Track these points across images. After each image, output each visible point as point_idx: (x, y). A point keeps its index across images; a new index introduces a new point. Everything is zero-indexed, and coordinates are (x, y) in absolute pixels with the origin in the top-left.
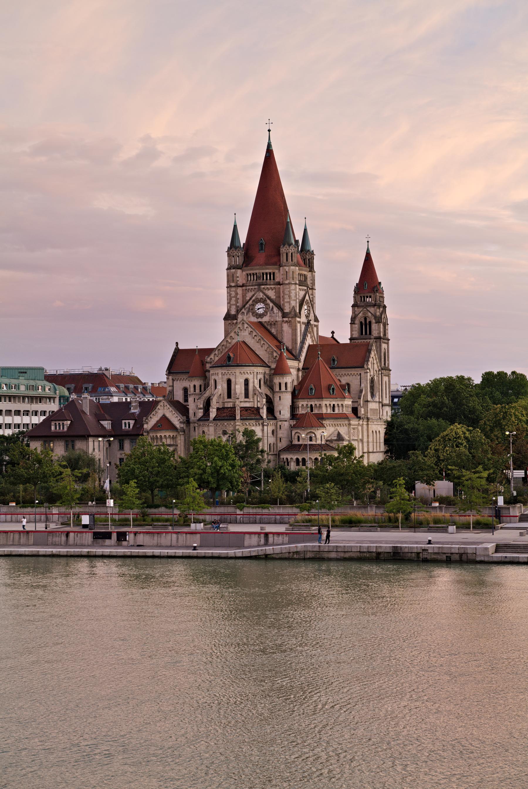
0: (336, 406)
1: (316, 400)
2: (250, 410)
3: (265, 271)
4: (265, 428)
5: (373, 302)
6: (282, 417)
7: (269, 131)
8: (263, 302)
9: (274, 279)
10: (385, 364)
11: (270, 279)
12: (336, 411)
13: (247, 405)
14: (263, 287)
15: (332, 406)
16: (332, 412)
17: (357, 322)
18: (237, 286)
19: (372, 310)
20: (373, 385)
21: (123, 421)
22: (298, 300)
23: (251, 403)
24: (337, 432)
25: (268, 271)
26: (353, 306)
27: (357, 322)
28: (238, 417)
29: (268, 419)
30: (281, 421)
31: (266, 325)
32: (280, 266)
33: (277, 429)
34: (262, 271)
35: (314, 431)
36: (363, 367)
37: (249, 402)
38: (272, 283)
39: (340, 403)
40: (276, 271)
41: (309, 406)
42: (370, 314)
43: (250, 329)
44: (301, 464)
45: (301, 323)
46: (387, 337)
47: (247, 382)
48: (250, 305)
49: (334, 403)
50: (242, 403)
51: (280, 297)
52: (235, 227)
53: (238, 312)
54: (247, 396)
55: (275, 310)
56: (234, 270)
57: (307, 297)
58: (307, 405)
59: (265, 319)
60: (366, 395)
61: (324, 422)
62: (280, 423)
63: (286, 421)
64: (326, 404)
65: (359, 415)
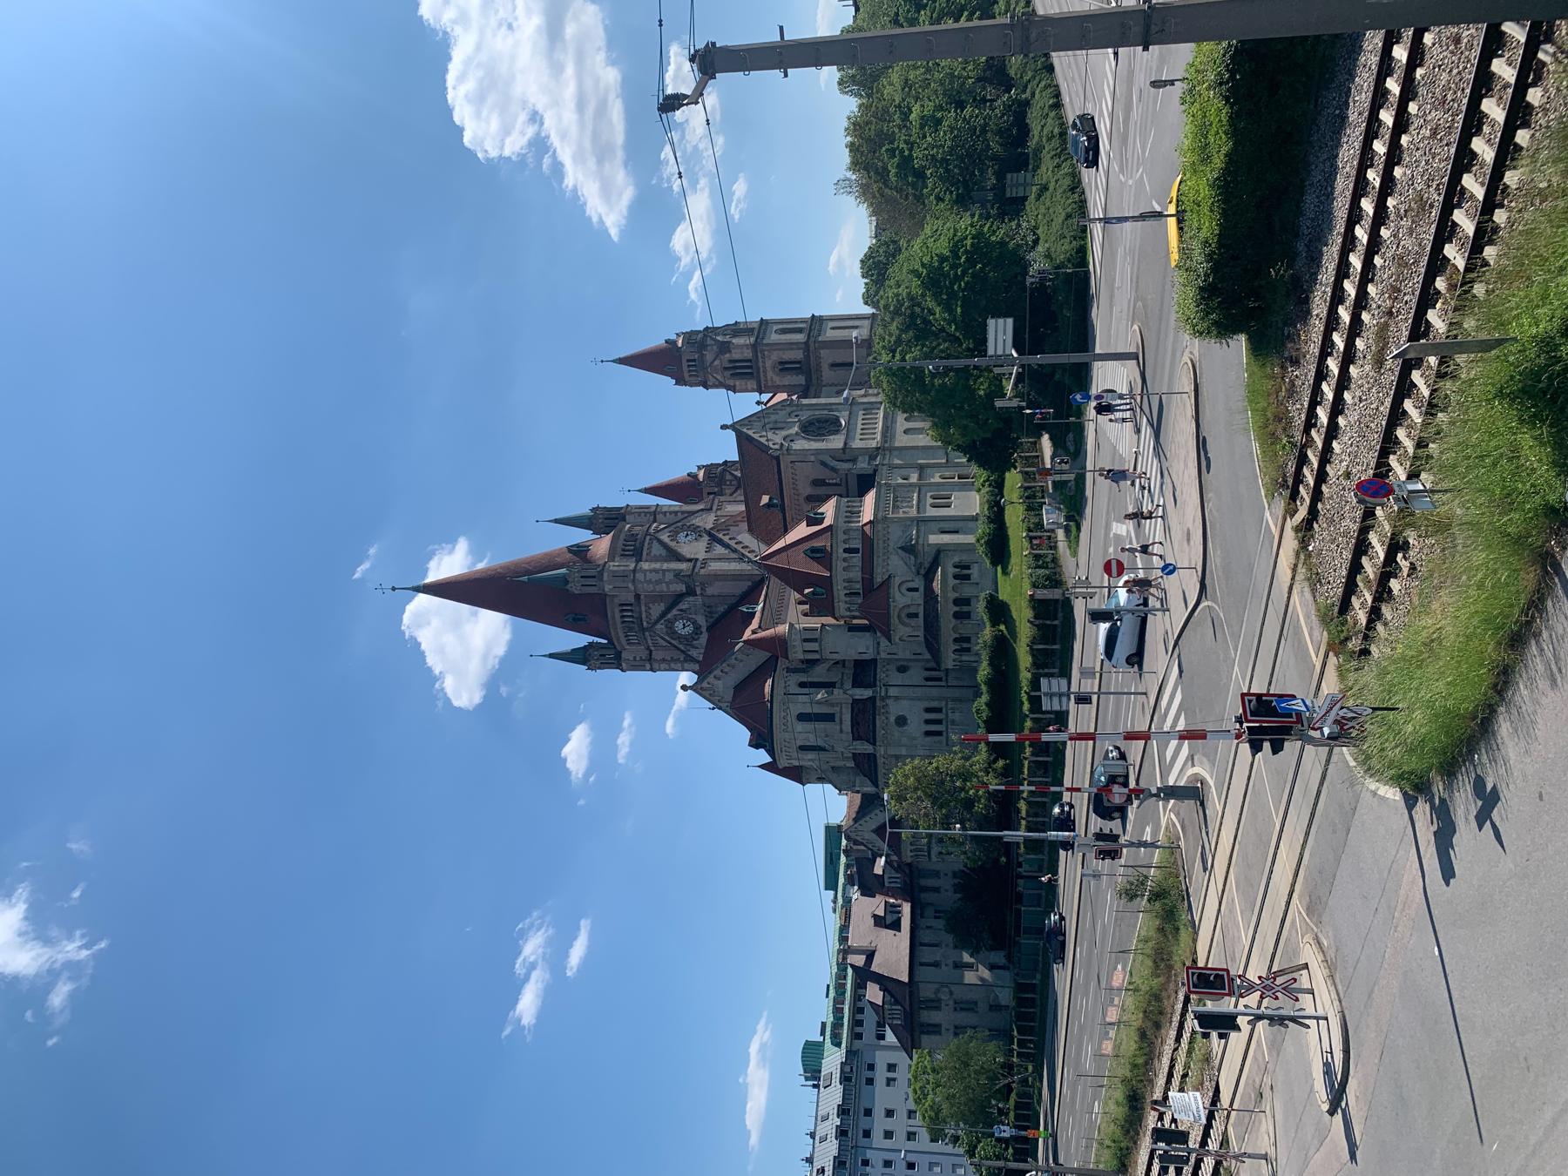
0: (847, 546)
1: (835, 589)
2: (857, 715)
3: (618, 620)
4: (893, 692)
5: (696, 356)
6: (871, 650)
7: (394, 589)
8: (673, 623)
9: (631, 605)
10: (800, 331)
11: (631, 611)
12: (860, 546)
13: (847, 717)
14: (645, 624)
15: (847, 555)
16: (860, 555)
17: (731, 382)
18: (650, 659)
19: (709, 356)
20: (819, 421)
21: (887, 884)
22: (665, 566)
23: (844, 710)
24: (900, 551)
25: (618, 615)
26: (706, 387)
27: (731, 382)
28: (868, 748)
29: (875, 686)
30: (878, 653)
31: (711, 620)
32: (606, 595)
33: (897, 660)
34: (619, 625)
35: (896, 614)
36: (777, 458)
37: (841, 713)
38: (637, 609)
39: (842, 537)
40: (617, 601)
41: (848, 599)
42: (717, 362)
43: (711, 679)
44: (965, 645)
45: (709, 555)
46: (756, 326)
47: (802, 717)
48: (681, 643)
49: (841, 550)
50: (844, 728)
51: (660, 597)
52: (551, 656)
53: (693, 660)
54: (829, 718)
55: (683, 606)
56: (624, 665)
57: (665, 537)
58: (846, 602)
59: (702, 621)
60: (833, 454)
61: (879, 579)
62: (883, 655)
63: (878, 643)
64: (844, 569)
65: (871, 472)
